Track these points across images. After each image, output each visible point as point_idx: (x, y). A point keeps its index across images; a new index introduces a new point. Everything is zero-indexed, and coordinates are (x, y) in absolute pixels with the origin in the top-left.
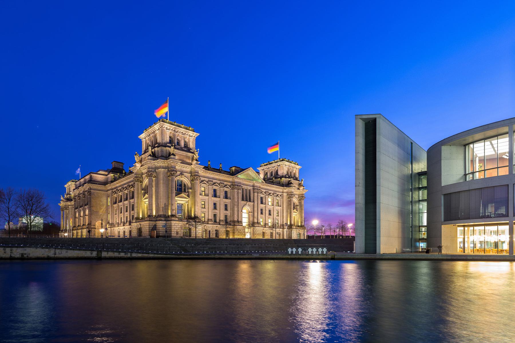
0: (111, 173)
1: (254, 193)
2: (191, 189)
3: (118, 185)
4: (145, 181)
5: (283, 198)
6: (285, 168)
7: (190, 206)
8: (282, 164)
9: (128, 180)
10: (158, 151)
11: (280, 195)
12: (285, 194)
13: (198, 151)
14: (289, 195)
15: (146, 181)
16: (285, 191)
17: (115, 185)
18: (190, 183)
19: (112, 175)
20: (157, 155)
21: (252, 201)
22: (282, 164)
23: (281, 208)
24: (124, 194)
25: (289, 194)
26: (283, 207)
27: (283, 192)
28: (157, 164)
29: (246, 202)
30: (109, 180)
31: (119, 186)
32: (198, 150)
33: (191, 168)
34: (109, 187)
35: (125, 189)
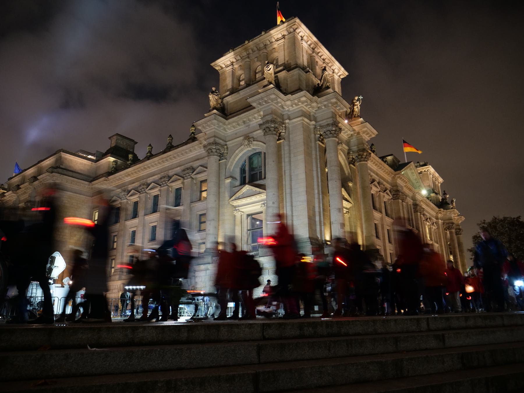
0: (110, 155)
2: (351, 181)
3: (128, 179)
4: (237, 155)
6: (430, 177)
7: (353, 224)
8: (425, 171)
9: (167, 164)
10: (285, 79)
13: (361, 101)
14: (448, 223)
15: (240, 155)
17: (121, 179)
18: (348, 167)
19: (111, 159)
20: (283, 87)
22: (426, 170)
24: (146, 198)
25: (447, 221)
28: (288, 106)
30: (102, 171)
31: (133, 182)
32: (361, 97)
33: (352, 133)
34: (101, 184)
35: (150, 186)
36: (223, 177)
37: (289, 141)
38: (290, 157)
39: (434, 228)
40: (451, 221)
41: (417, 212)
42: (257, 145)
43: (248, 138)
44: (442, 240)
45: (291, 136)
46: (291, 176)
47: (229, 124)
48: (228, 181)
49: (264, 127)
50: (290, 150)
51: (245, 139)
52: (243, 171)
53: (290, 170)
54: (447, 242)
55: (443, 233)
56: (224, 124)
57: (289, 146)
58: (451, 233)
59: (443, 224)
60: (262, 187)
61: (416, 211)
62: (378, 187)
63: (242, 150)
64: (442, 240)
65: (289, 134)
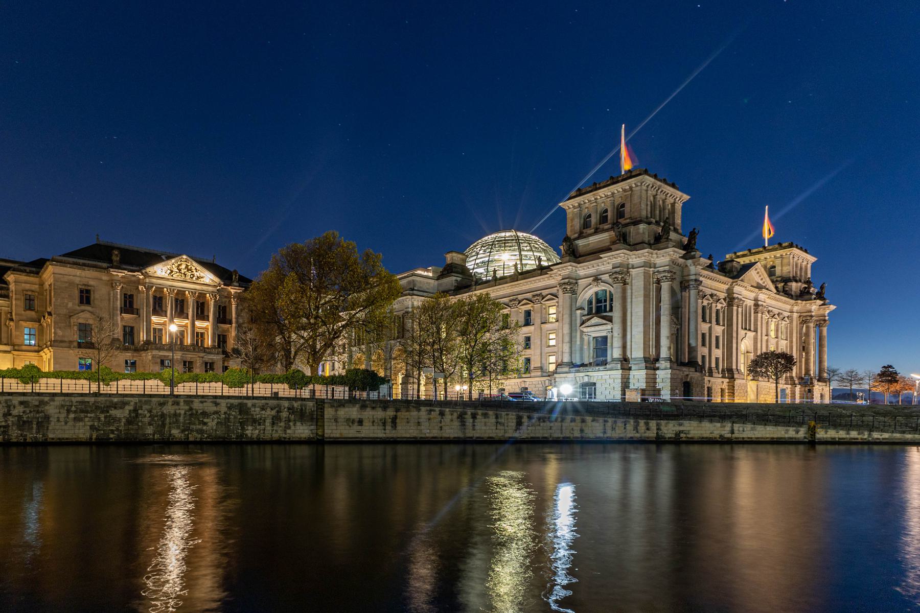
1: (756, 312)
5: (791, 322)
9: (516, 290)
11: (788, 317)
12: (795, 315)
16: (795, 308)
21: (752, 329)
23: (787, 344)
26: (791, 342)
27: (792, 312)
29: (746, 331)
36: (574, 309)
37: (632, 286)
38: (632, 298)
39: (784, 322)
40: (809, 314)
41: (757, 313)
42: (603, 286)
43: (597, 279)
44: (794, 335)
45: (633, 281)
46: (631, 313)
47: (581, 267)
48: (579, 312)
49: (614, 276)
50: (632, 293)
51: (594, 280)
52: (590, 302)
53: (632, 308)
54: (801, 338)
55: (797, 327)
56: (576, 267)
57: (632, 289)
58: (808, 327)
59: (800, 316)
60: (610, 320)
61: (756, 312)
62: (711, 299)
63: (591, 288)
64: (794, 335)
65: (632, 280)
